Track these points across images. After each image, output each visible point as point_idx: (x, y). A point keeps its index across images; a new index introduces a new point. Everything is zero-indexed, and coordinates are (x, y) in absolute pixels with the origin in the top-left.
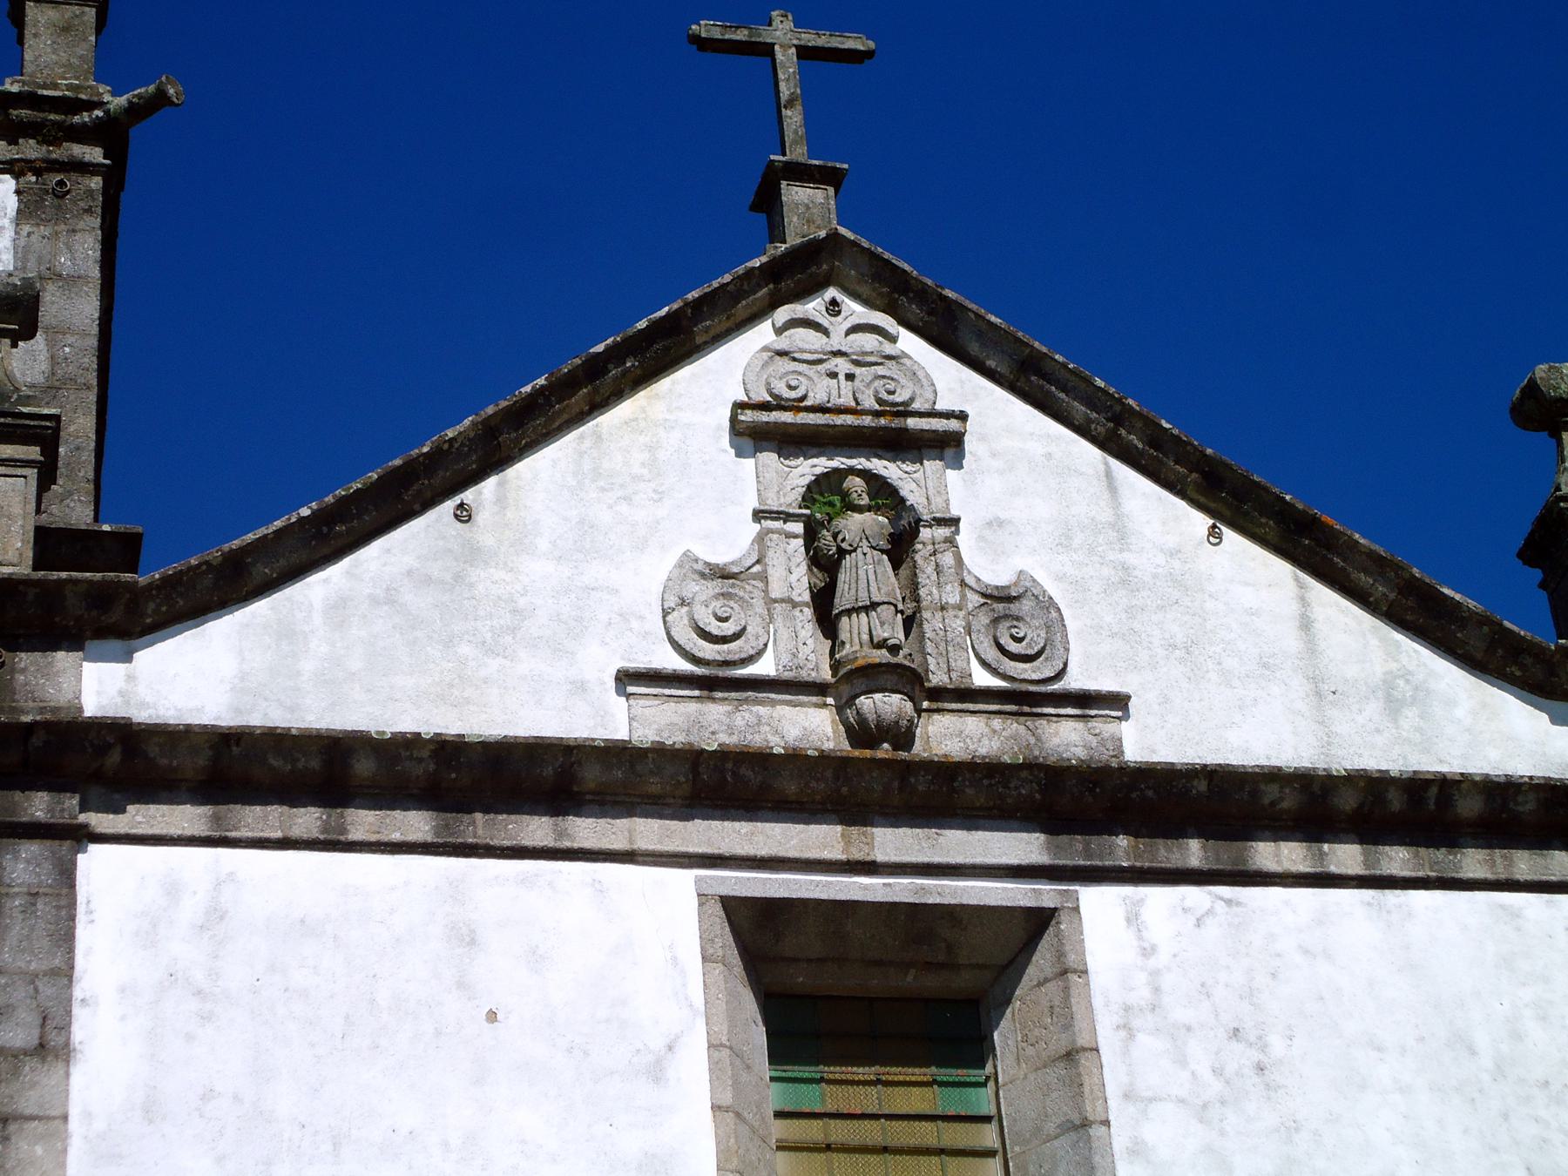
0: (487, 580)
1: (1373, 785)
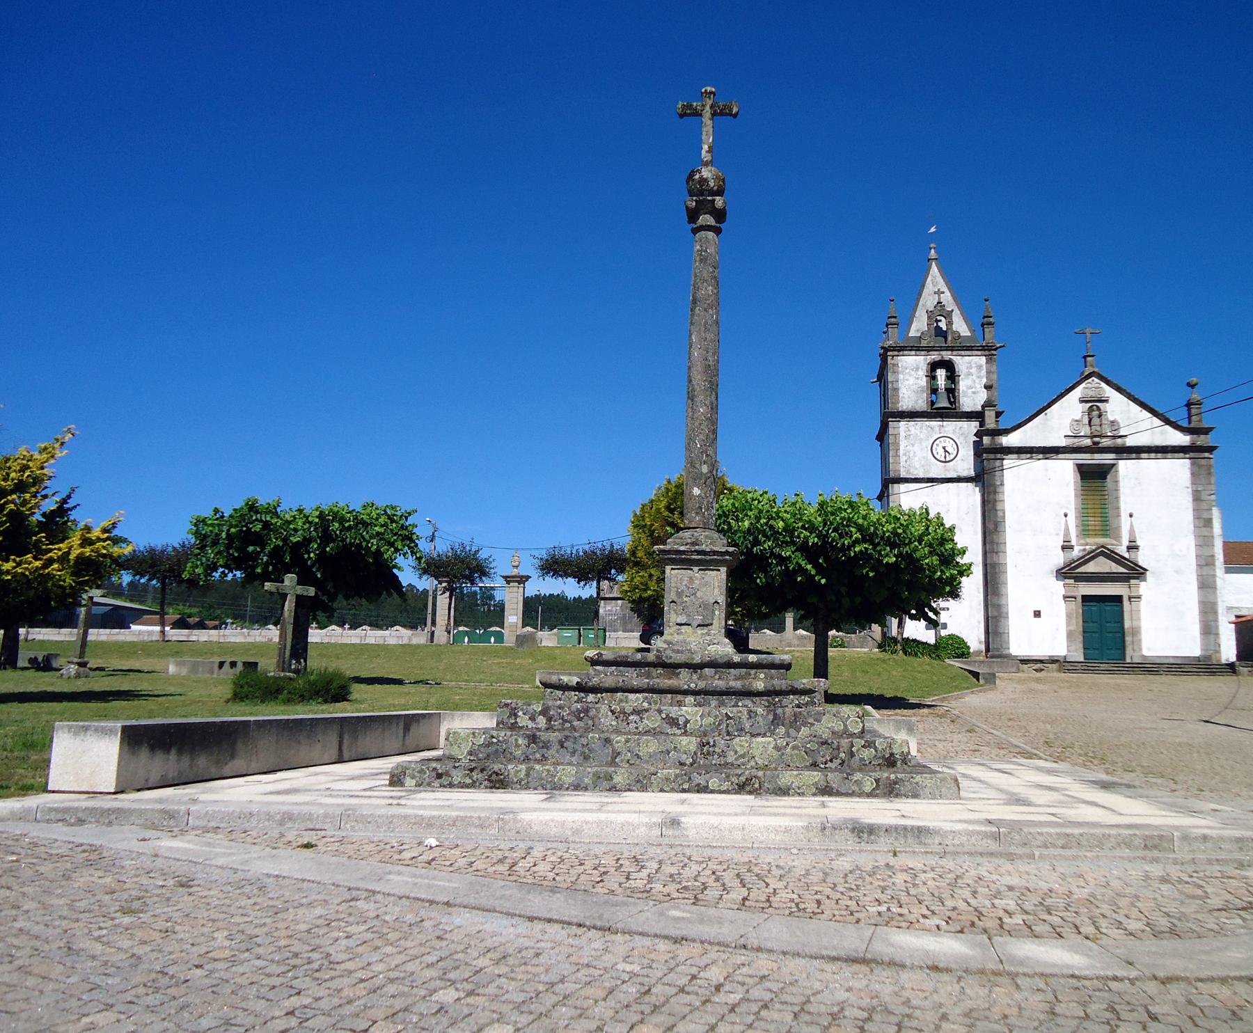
0: (1049, 423)
1: (1157, 447)
